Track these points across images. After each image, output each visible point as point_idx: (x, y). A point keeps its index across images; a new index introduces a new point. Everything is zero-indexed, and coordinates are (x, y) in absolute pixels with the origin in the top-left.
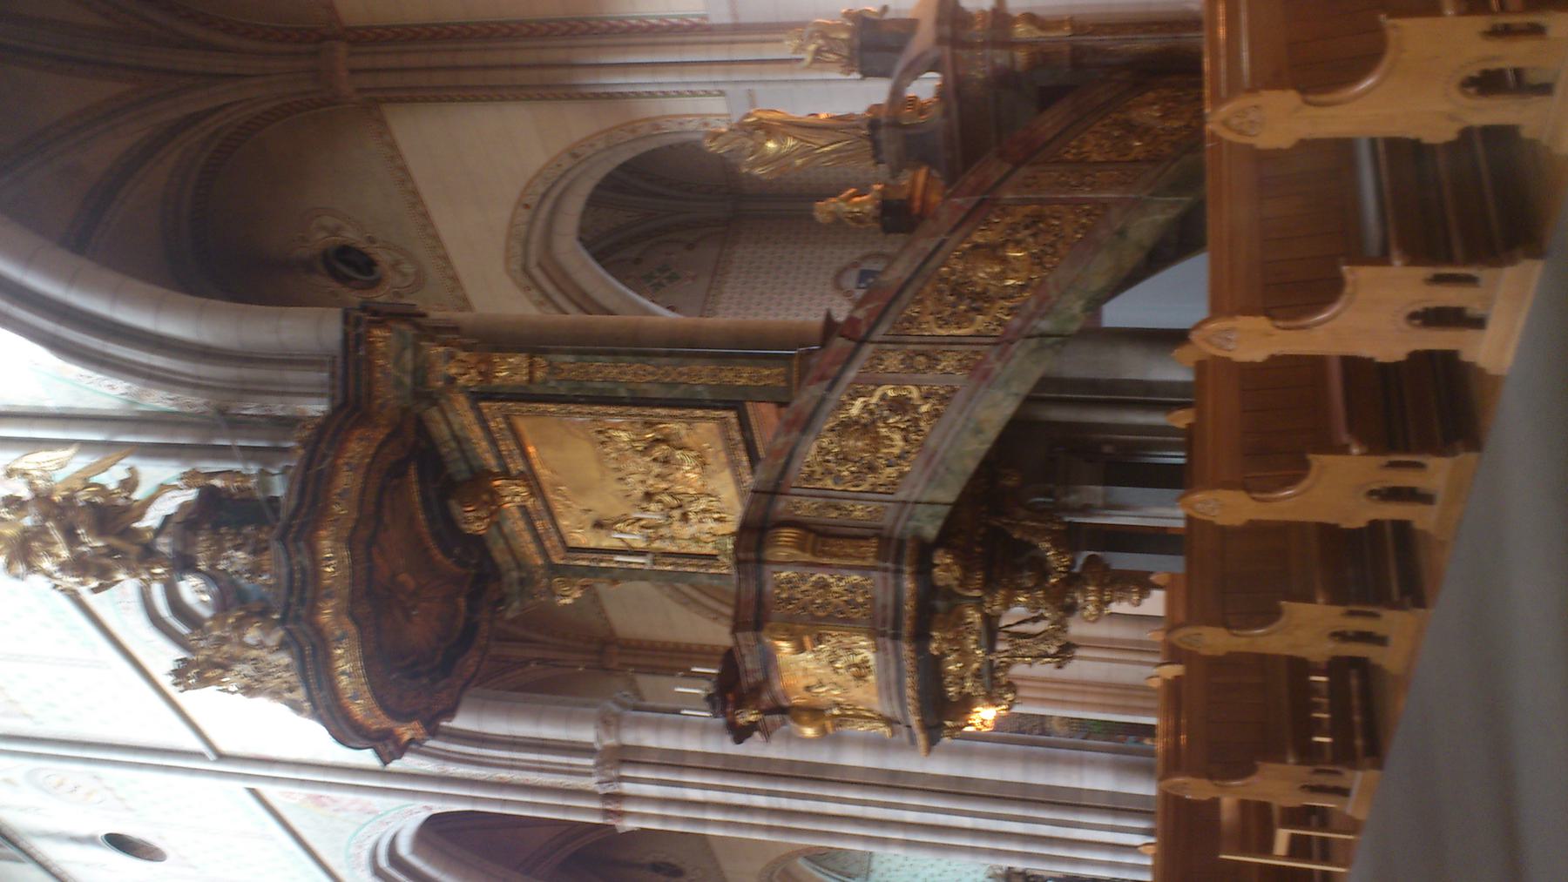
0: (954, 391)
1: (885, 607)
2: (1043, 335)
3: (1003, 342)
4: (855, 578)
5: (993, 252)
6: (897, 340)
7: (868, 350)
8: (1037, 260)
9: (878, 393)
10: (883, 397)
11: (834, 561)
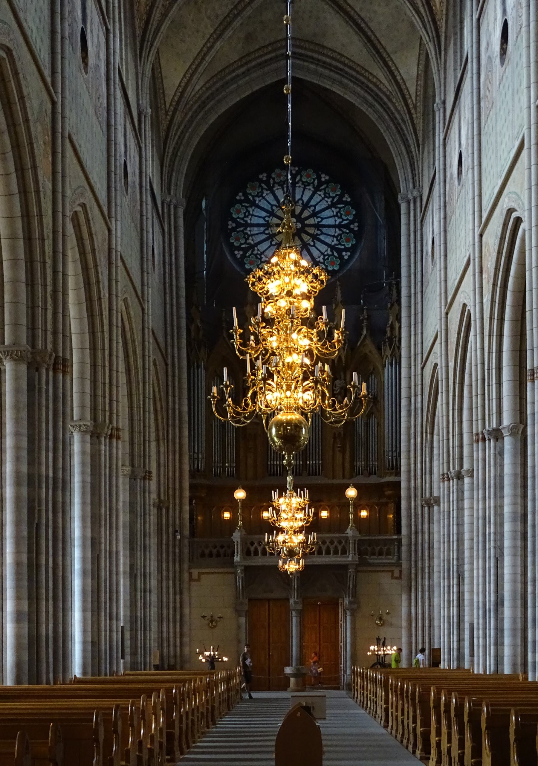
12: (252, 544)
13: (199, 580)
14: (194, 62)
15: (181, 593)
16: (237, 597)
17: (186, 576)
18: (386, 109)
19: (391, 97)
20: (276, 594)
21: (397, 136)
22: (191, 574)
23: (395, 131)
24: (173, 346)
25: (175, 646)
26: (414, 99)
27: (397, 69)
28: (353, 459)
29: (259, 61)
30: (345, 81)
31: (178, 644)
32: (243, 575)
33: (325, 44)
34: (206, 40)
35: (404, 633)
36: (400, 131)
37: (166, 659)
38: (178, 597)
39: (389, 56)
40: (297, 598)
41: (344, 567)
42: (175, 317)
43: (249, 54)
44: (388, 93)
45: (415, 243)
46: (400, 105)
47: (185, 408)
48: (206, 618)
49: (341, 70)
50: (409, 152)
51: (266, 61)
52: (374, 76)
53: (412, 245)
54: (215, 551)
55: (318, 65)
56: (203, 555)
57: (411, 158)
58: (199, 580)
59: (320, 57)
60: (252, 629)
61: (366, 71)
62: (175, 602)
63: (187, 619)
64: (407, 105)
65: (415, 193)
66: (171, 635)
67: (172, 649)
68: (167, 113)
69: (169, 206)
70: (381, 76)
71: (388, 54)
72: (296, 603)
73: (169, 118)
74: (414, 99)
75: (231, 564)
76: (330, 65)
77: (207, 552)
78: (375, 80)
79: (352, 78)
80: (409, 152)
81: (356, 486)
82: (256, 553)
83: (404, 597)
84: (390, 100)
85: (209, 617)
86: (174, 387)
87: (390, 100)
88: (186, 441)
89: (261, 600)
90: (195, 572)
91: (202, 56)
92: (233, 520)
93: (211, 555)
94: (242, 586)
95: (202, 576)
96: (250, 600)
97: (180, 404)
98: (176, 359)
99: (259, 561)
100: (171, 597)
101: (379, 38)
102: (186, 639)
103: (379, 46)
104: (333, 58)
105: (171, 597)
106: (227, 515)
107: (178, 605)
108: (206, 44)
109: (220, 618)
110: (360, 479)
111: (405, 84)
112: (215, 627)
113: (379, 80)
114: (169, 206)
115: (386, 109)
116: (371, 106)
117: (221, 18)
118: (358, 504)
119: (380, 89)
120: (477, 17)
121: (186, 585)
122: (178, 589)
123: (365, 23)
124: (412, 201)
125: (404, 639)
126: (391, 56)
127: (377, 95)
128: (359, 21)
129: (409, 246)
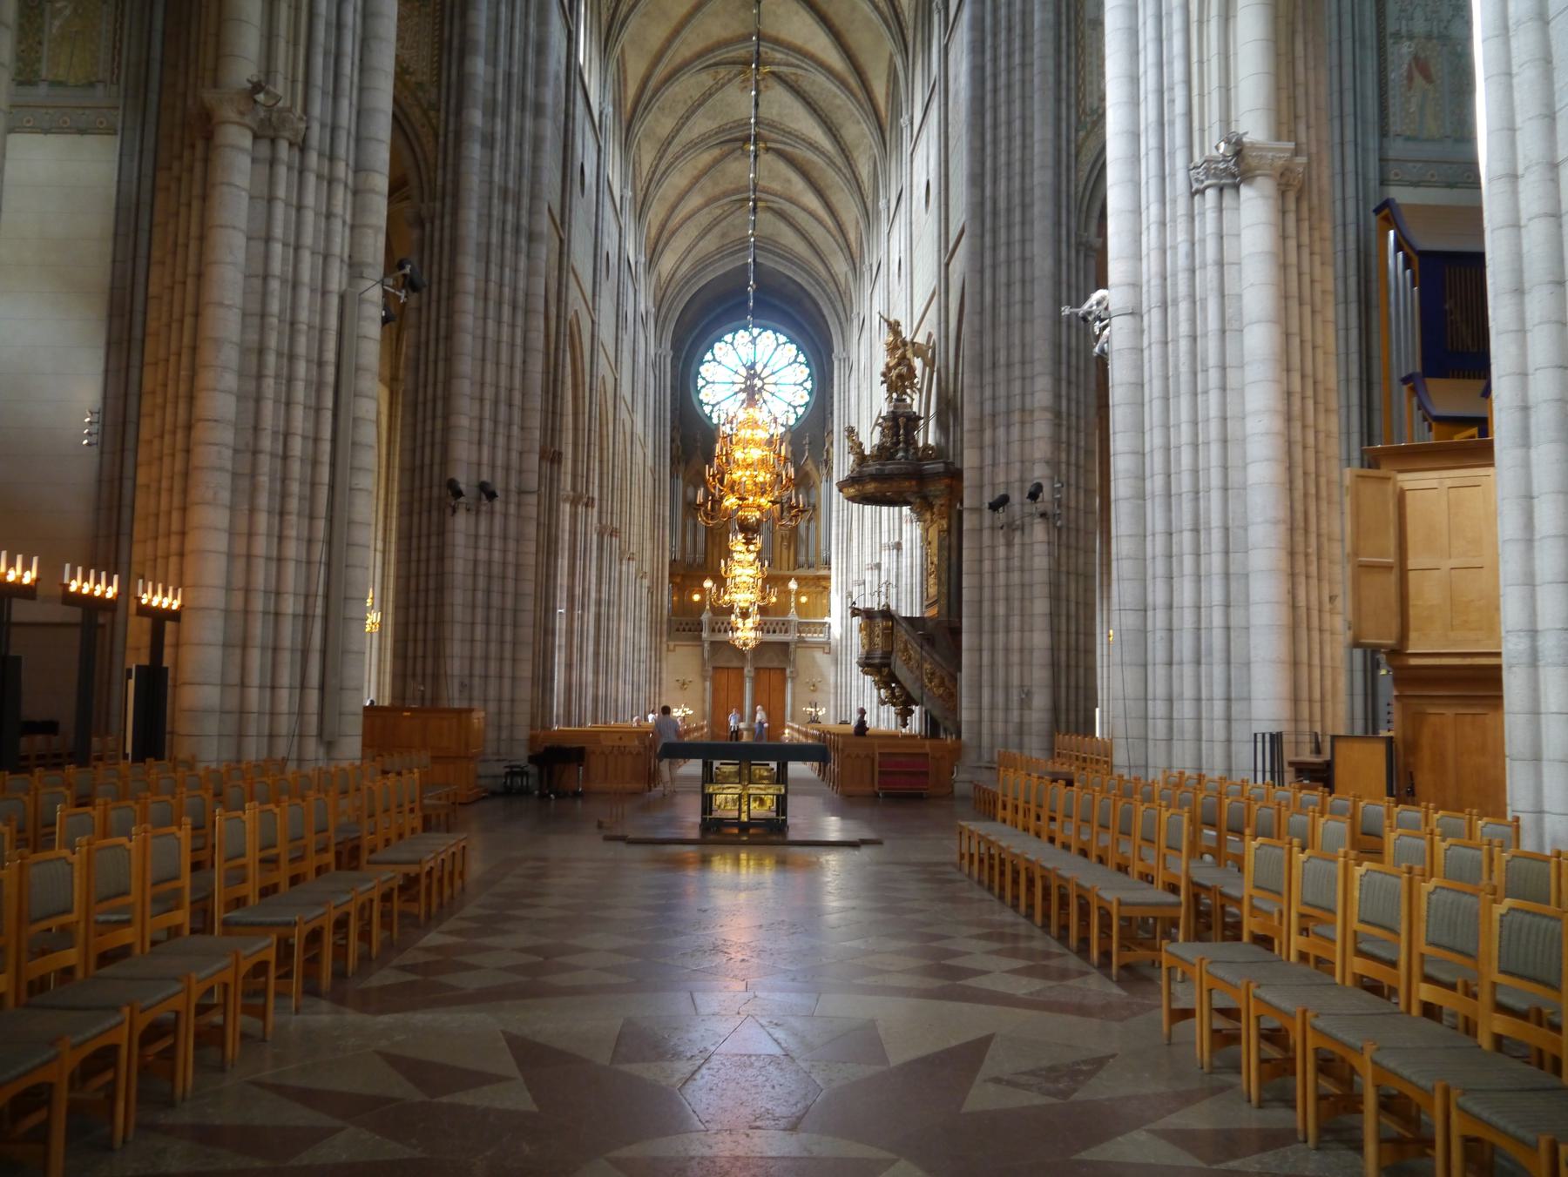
3: (922, 687)
5: (942, 684)
6: (922, 657)
8: (940, 696)
16: (704, 665)
17: (664, 646)
18: (825, 291)
20: (735, 664)
28: (796, 554)
35: (832, 697)
36: (834, 307)
41: (786, 644)
46: (835, 290)
47: (668, 514)
50: (840, 323)
56: (678, 630)
63: (664, 682)
70: (821, 268)
75: (700, 637)
79: (799, 266)
80: (840, 323)
81: (798, 579)
82: (720, 631)
83: (832, 669)
89: (722, 668)
90: (672, 644)
91: (689, 251)
92: (702, 602)
96: (714, 668)
99: (720, 637)
110: (802, 572)
115: (825, 291)
118: (798, 594)
121: (664, 654)
125: (832, 703)
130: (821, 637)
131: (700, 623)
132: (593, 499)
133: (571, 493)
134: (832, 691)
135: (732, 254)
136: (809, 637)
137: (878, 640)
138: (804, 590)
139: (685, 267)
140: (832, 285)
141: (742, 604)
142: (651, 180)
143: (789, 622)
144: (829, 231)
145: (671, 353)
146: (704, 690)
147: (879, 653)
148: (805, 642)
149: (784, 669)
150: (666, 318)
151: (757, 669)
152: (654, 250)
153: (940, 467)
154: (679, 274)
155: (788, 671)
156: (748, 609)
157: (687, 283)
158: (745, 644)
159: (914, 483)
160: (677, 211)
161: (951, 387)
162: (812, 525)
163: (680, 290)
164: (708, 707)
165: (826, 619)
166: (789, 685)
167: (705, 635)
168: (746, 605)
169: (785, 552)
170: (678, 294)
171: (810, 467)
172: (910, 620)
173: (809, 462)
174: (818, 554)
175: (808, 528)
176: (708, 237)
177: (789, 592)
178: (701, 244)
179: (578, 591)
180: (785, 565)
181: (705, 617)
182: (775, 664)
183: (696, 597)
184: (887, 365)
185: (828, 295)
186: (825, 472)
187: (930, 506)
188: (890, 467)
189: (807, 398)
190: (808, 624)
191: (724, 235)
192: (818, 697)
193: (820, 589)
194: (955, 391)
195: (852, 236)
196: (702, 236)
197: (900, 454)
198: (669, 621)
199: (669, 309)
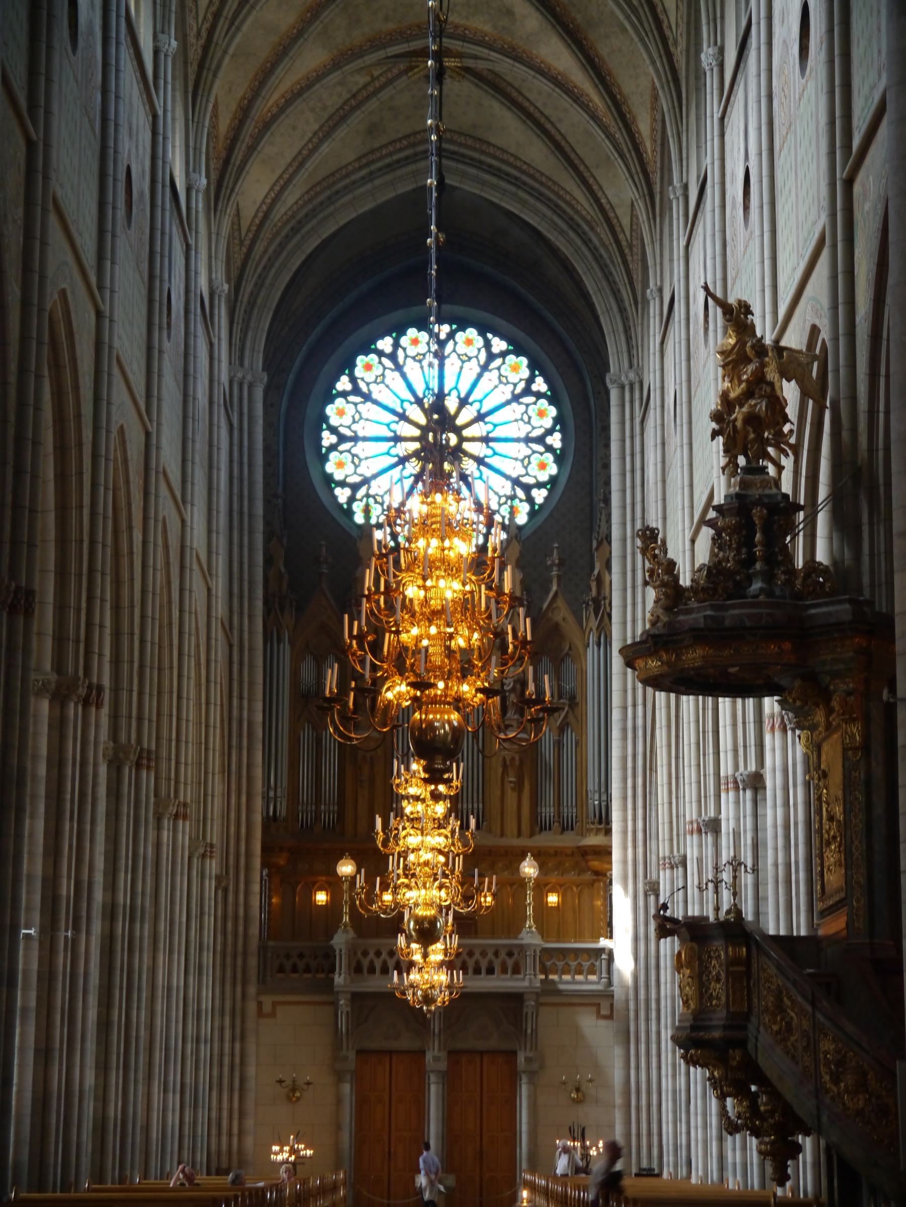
0: (797, 1063)
1: (711, 1020)
2: (819, 1118)
4: (724, 999)
7: (809, 1008)
9: (792, 1014)
10: (792, 1018)
11: (730, 985)
12: (365, 954)
13: (273, 1015)
14: (287, 169)
15: (243, 1038)
17: (252, 1007)
18: (587, 242)
19: (594, 224)
20: (406, 1042)
21: (604, 283)
22: (260, 1004)
23: (600, 274)
24: (241, 614)
25: (230, 1134)
26: (628, 234)
27: (601, 188)
28: (535, 802)
29: (388, 161)
30: (521, 194)
31: (235, 1130)
32: (349, 1009)
33: (492, 140)
34: (306, 139)
36: (608, 277)
37: (214, 1157)
38: (238, 1046)
39: (589, 170)
40: (439, 1049)
42: (246, 566)
43: (372, 151)
44: (589, 218)
45: (633, 455)
46: (608, 238)
47: (259, 717)
48: (283, 1084)
49: (516, 178)
50: (622, 310)
51: (398, 161)
52: (567, 192)
53: (628, 459)
54: (301, 965)
55: (480, 168)
56: (281, 970)
57: (625, 320)
58: (273, 1015)
59: (483, 158)
60: (362, 1104)
61: (555, 183)
62: (232, 1055)
63: (251, 1084)
64: (617, 241)
65: (632, 375)
66: (225, 1114)
67: (224, 1139)
68: (241, 243)
69: (241, 385)
71: (586, 166)
72: (436, 1059)
73: (244, 250)
74: (628, 234)
75: (328, 986)
76: (499, 170)
77: (288, 965)
78: (568, 198)
80: (622, 310)
81: (540, 856)
82: (372, 970)
84: (592, 228)
85: (289, 1082)
86: (241, 682)
87: (592, 228)
88: (259, 772)
90: (267, 1001)
91: (300, 161)
93: (294, 970)
94: (347, 1029)
95: (280, 1010)
96: (360, 1052)
97: (250, 710)
98: (246, 636)
99: (373, 984)
100: (227, 1045)
101: (573, 145)
102: (250, 1123)
103: (573, 156)
104: (503, 161)
105: (227, 1045)
106: (321, 897)
107: (237, 1060)
108: (306, 145)
109: (308, 1084)
110: (548, 840)
111: (614, 211)
112: (298, 1099)
113: (574, 198)
114: (241, 385)
115: (587, 242)
116: (562, 232)
117: (331, 110)
118: (542, 888)
119: (577, 212)
120: (719, 115)
121: (250, 1024)
122: (238, 1031)
123: (552, 123)
124: (627, 389)
126: (592, 170)
127: (572, 219)
128: (543, 120)
129: (623, 458)
130: (592, 982)
131: (329, 955)
132: (100, 689)
133: (53, 677)
134: (618, 1100)
135: (390, 167)
136: (567, 982)
137: (717, 988)
138: (553, 878)
139: (292, 197)
140: (603, 230)
141: (420, 912)
142: (217, 16)
143: (522, 948)
144: (594, 117)
145: (265, 377)
146: (339, 1101)
147: (719, 1017)
148: (559, 992)
149: (514, 1053)
150: (252, 304)
151: (454, 1055)
152: (227, 162)
153: (842, 610)
154: (281, 210)
155: (521, 1058)
156: (433, 921)
157: (295, 231)
158: (428, 999)
159: (787, 646)
160: (273, 80)
161: (863, 440)
162: (569, 737)
163: (282, 246)
164: (346, 1139)
165: (604, 942)
166: (524, 1090)
167: (339, 979)
168: (431, 912)
169: (511, 798)
170: (277, 253)
171: (562, 614)
172: (787, 943)
173: (560, 602)
174: (581, 795)
175: (559, 744)
176: (341, 133)
177: (522, 883)
178: (325, 148)
179: (66, 888)
180: (511, 825)
181: (340, 940)
182: (493, 1043)
183: (321, 897)
184: (724, 396)
185: (593, 250)
186: (594, 623)
187: (824, 697)
188: (734, 613)
189: (553, 469)
190: (564, 952)
191: (372, 130)
192: (588, 1114)
193: (588, 876)
194: (872, 449)
195: (644, 127)
196: (327, 131)
197: (757, 585)
198: (263, 948)
199: (259, 285)
